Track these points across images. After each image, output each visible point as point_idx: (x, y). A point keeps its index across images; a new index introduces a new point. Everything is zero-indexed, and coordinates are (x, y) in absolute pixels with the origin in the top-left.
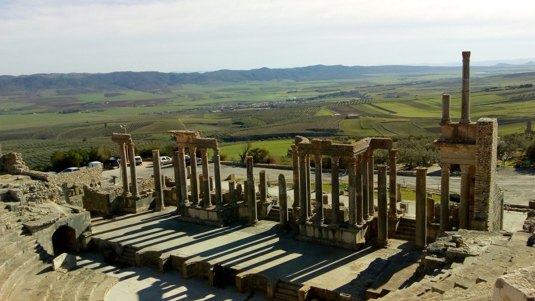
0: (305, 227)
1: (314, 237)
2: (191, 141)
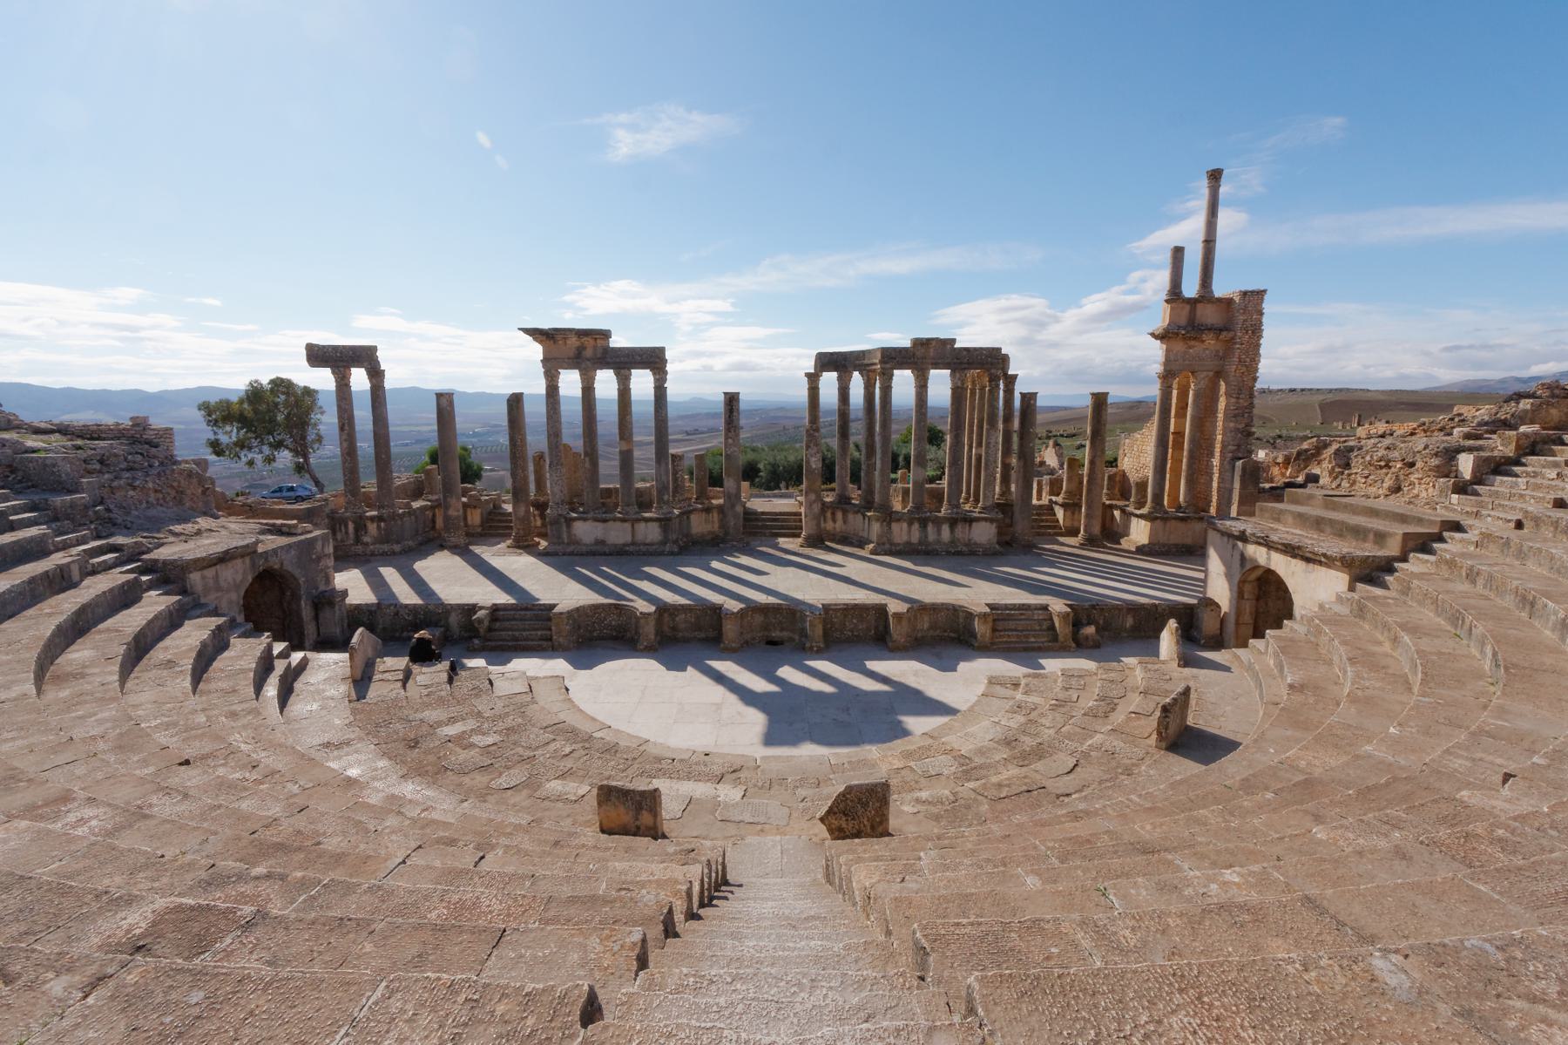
0: (889, 525)
1: (909, 543)
2: (588, 353)
